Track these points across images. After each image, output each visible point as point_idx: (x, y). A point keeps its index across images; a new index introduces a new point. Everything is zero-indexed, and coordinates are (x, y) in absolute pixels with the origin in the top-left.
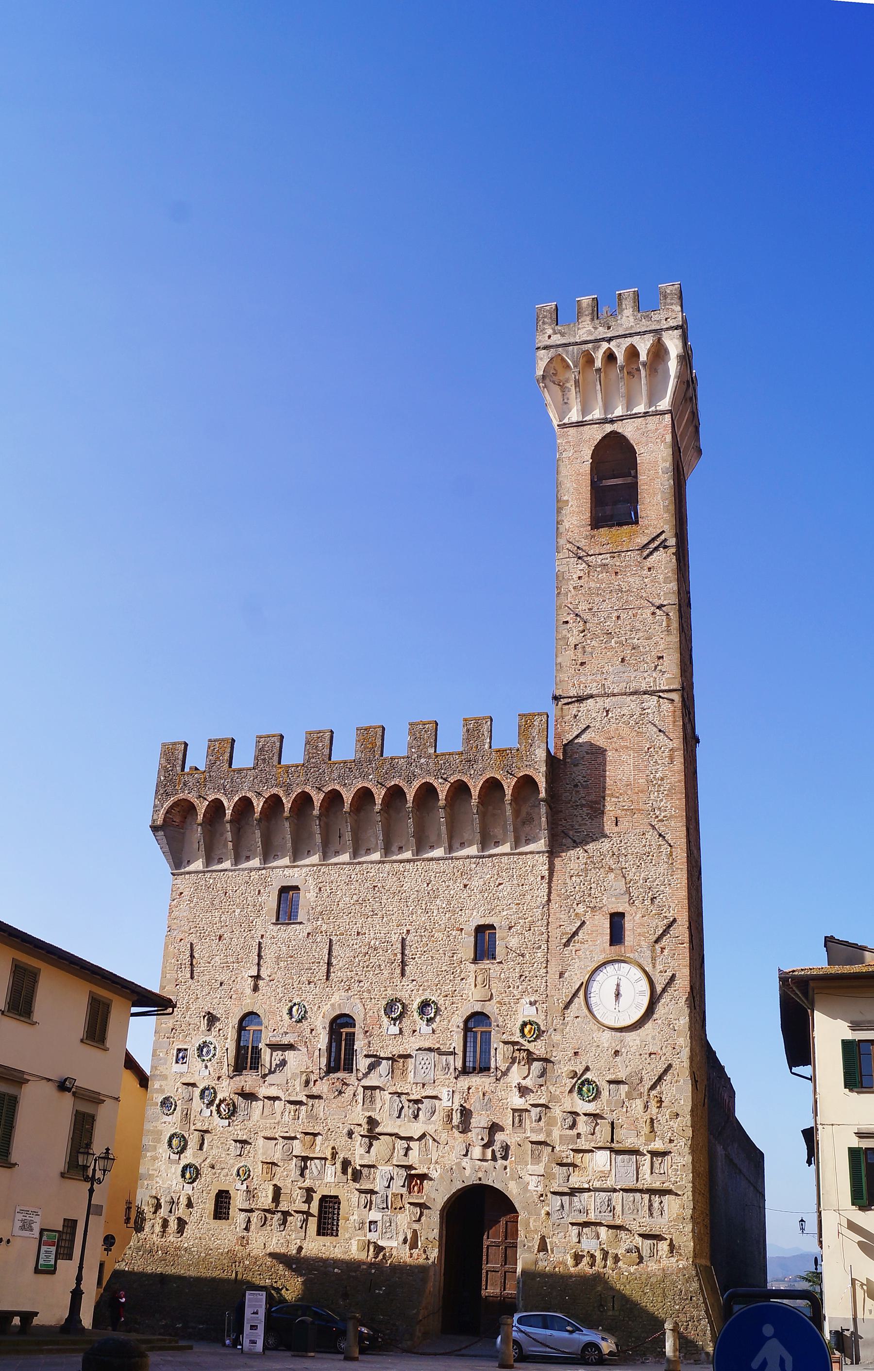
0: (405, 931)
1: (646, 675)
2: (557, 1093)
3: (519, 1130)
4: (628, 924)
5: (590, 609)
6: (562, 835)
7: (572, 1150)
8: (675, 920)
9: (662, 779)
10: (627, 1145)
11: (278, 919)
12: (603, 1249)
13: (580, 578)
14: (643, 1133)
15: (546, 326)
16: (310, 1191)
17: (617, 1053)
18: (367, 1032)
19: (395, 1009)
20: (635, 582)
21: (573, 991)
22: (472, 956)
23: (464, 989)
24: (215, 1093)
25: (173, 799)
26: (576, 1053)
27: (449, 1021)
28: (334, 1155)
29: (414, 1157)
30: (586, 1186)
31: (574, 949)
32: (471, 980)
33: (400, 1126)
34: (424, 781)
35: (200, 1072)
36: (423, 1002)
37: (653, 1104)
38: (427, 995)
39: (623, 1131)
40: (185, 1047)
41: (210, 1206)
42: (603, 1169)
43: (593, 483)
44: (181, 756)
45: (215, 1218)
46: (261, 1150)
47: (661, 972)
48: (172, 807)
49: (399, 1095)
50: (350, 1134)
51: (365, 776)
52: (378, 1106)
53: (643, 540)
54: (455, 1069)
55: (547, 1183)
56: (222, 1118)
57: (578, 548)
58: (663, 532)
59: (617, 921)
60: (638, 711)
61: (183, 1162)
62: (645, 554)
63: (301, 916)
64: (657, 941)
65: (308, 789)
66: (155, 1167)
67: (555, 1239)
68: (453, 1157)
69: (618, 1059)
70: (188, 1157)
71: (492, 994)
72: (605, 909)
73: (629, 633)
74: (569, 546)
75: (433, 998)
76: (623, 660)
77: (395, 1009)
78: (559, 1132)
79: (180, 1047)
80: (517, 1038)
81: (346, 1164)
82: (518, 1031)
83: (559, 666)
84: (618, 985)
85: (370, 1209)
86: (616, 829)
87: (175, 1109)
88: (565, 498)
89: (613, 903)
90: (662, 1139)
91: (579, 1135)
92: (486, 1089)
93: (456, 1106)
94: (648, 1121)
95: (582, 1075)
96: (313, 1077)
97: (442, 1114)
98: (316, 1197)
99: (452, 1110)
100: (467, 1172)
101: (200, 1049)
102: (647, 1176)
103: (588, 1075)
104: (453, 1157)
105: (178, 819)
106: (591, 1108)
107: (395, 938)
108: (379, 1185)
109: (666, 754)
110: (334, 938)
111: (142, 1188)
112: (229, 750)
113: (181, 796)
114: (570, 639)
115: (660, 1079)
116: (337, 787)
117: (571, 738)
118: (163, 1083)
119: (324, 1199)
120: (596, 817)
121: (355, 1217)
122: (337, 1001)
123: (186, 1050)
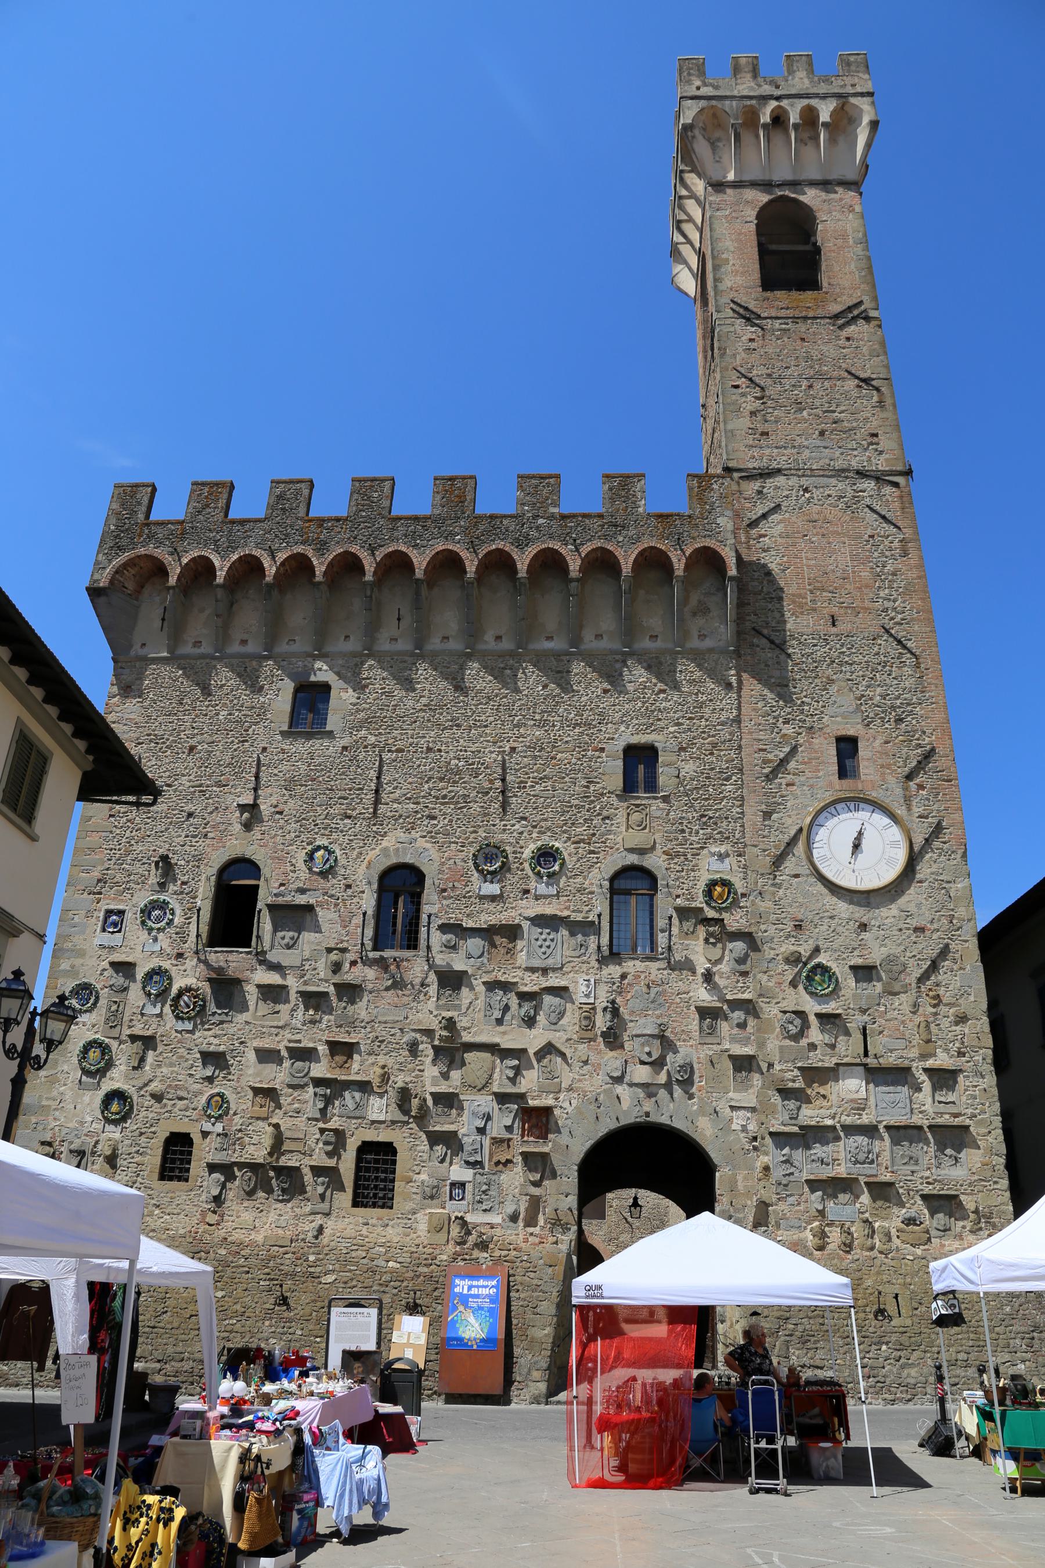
0: (507, 749)
1: (855, 453)
2: (770, 984)
3: (709, 1040)
4: (864, 751)
5: (769, 375)
6: (753, 632)
7: (799, 1068)
8: (933, 750)
9: (894, 574)
10: (891, 1060)
11: (290, 727)
12: (866, 1221)
13: (751, 340)
14: (915, 1042)
15: (693, 78)
16: (340, 1135)
17: (864, 927)
18: (444, 890)
19: (492, 860)
20: (830, 351)
21: (786, 838)
22: (620, 784)
23: (609, 832)
24: (170, 978)
25: (126, 556)
26: (798, 927)
27: (585, 879)
28: (385, 1078)
29: (530, 1081)
30: (829, 1122)
31: (784, 781)
32: (621, 818)
33: (504, 1033)
34: (543, 546)
35: (142, 948)
36: (539, 849)
37: (924, 1001)
38: (546, 840)
39: (883, 1039)
40: (121, 907)
41: (154, 1159)
42: (855, 1096)
43: (761, 246)
44: (145, 501)
45: (162, 1178)
46: (251, 1072)
47: (920, 817)
48: (125, 566)
49: (506, 987)
50: (413, 1048)
51: (449, 536)
52: (465, 1002)
53: (836, 308)
54: (599, 947)
55: (763, 1118)
56: (182, 1019)
57: (746, 309)
58: (861, 303)
59: (847, 748)
60: (850, 493)
61: (108, 1085)
62: (841, 322)
63: (333, 722)
64: (909, 777)
65: (354, 549)
66: (55, 1093)
67: (782, 1206)
68: (596, 1084)
69: (865, 935)
70: (116, 1080)
71: (655, 842)
72: (827, 730)
73: (827, 405)
74: (732, 305)
75: (557, 845)
76: (822, 433)
77: (492, 860)
78: (777, 1043)
79: (111, 907)
80: (700, 902)
81: (404, 1096)
82: (701, 895)
83: (730, 434)
84: (860, 834)
85: (451, 1164)
86: (834, 630)
87: (95, 1004)
88: (724, 256)
89: (839, 723)
90: (947, 1050)
91: (812, 1047)
92: (652, 977)
93: (602, 1002)
94: (923, 1025)
95: (810, 958)
96: (350, 956)
97: (577, 1015)
98: (352, 1145)
99: (594, 1009)
100: (626, 1104)
101: (146, 912)
102: (928, 1107)
103: (822, 959)
104: (596, 1084)
105: (131, 586)
106: (831, 1007)
107: (491, 757)
108: (464, 1126)
109: (896, 544)
110: (386, 756)
111: (27, 1127)
112: (225, 496)
113: (142, 551)
114: (744, 405)
115: (934, 966)
116: (404, 549)
117: (754, 517)
118: (78, 962)
119: (366, 1148)
120: (802, 613)
121: (424, 1177)
122: (394, 845)
123: (121, 913)
